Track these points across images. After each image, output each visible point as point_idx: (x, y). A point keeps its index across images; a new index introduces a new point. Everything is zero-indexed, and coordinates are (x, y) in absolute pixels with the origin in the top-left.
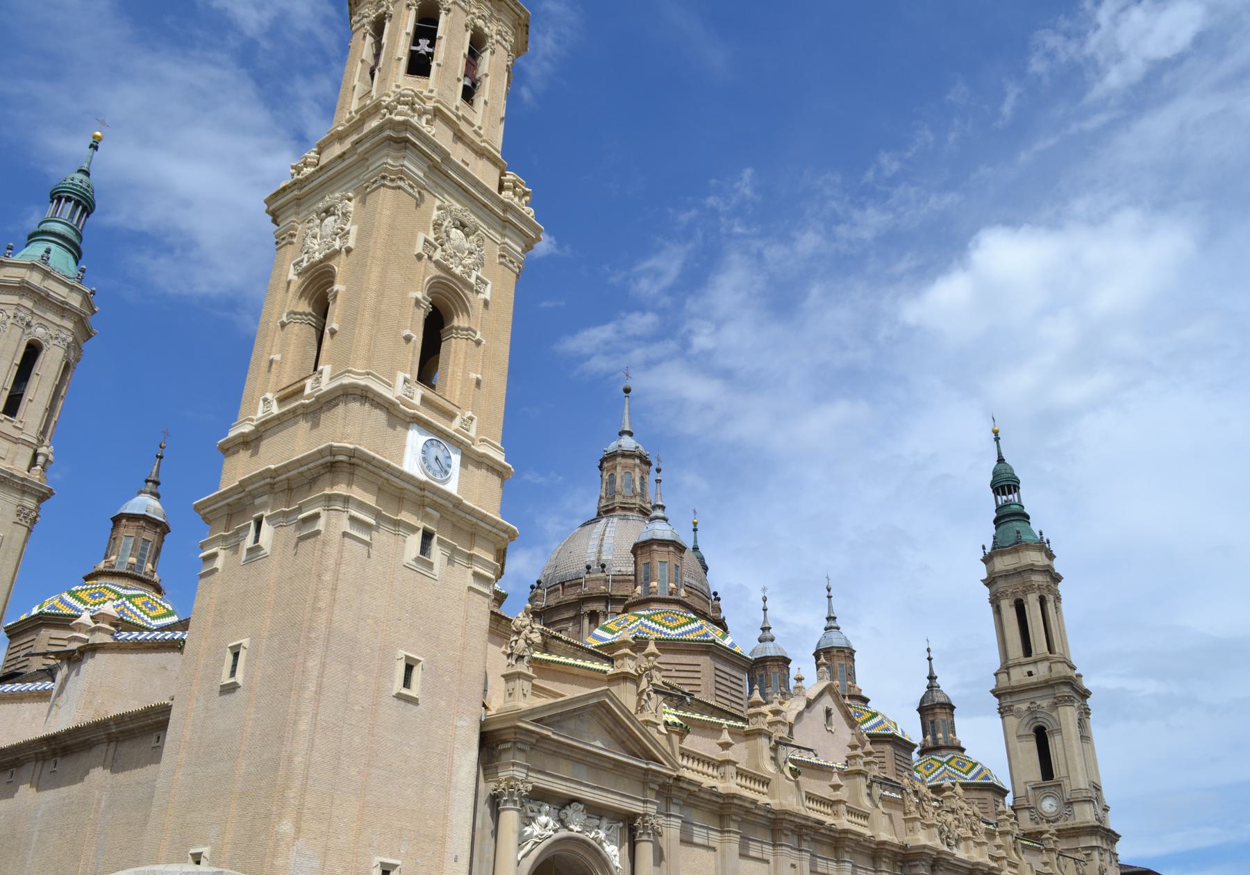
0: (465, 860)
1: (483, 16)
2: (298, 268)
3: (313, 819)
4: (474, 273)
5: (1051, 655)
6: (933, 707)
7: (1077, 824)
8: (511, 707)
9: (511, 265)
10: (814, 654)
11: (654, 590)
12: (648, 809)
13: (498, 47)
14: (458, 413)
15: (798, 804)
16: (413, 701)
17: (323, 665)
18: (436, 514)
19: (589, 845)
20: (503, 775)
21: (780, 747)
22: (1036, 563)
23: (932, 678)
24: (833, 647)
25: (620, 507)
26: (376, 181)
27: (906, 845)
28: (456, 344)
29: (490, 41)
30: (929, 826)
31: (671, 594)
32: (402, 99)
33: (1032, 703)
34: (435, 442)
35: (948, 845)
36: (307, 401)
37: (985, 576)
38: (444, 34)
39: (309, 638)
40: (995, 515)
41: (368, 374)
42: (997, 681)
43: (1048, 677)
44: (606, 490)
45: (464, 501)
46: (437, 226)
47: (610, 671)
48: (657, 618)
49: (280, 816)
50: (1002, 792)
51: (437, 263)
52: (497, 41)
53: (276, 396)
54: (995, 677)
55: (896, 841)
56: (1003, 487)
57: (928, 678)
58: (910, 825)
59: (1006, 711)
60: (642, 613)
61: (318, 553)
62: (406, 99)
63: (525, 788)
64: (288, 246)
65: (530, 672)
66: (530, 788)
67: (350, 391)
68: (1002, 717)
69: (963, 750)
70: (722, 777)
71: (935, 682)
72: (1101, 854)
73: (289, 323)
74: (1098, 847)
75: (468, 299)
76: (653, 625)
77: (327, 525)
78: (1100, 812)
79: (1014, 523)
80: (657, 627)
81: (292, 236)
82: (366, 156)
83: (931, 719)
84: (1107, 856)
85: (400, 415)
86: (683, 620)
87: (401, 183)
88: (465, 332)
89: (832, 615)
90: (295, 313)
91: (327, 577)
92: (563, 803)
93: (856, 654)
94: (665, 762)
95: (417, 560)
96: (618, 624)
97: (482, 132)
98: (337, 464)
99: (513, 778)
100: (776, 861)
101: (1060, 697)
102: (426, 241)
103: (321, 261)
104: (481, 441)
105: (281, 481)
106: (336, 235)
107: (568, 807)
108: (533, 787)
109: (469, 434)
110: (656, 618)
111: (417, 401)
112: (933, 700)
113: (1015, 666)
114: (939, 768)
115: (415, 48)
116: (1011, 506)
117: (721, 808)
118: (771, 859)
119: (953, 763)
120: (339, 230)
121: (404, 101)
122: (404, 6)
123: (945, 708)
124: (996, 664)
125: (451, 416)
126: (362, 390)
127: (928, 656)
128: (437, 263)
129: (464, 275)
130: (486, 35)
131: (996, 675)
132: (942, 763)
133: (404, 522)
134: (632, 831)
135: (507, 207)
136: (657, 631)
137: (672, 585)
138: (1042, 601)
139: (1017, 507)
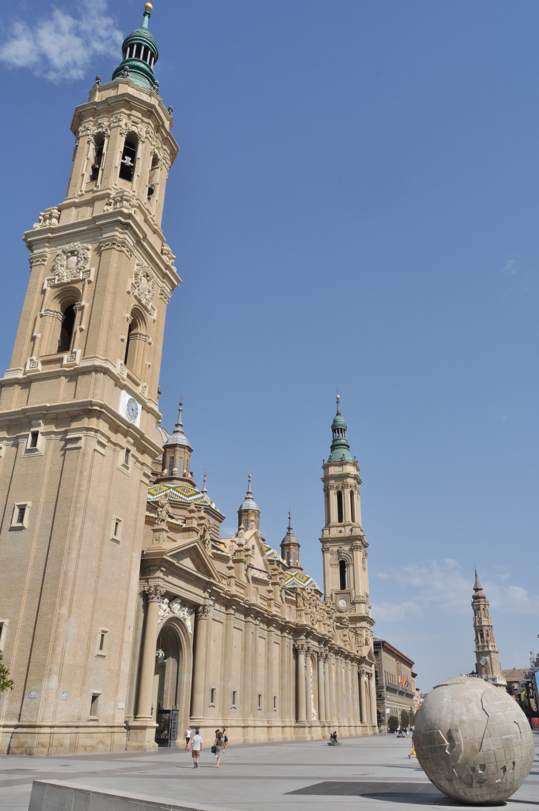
0: (132, 629)
1: (158, 147)
2: (51, 283)
3: (76, 607)
4: (151, 304)
5: (353, 523)
6: (289, 545)
7: (356, 614)
8: (158, 547)
9: (165, 300)
10: (238, 512)
11: (175, 473)
12: (206, 603)
13: (163, 167)
14: (141, 384)
15: (256, 600)
16: (118, 542)
17: (83, 523)
18: (132, 441)
19: (181, 621)
20: (152, 583)
21: (250, 569)
22: (351, 473)
24: (250, 509)
26: (109, 244)
27: (297, 624)
28: (139, 343)
29: (160, 163)
30: (306, 614)
31: (184, 476)
32: (124, 197)
33: (340, 548)
34: (132, 400)
35: (312, 624)
36: (67, 369)
37: (322, 476)
38: (141, 156)
39: (75, 507)
40: (331, 444)
41: (107, 360)
42: (323, 534)
43: (350, 535)
45: (145, 435)
46: (136, 275)
47: (184, 526)
48: (178, 489)
49: (61, 605)
50: (321, 594)
51: (136, 297)
52: (163, 164)
53: (41, 360)
55: (293, 621)
56: (338, 429)
58: (299, 612)
59: (326, 550)
60: (170, 485)
61: (80, 460)
62: (127, 198)
63: (163, 591)
64: (42, 266)
65: (166, 528)
66: (165, 591)
67: (98, 369)
68: (323, 553)
69: (302, 569)
70: (228, 585)
72: (367, 631)
74: (366, 628)
75: (147, 318)
76: (177, 494)
77: (86, 444)
78: (367, 609)
79: (342, 449)
80: (179, 495)
81: (44, 260)
82: (101, 227)
83: (288, 551)
84: (369, 632)
85: (119, 384)
86: (193, 493)
87: (123, 249)
88: (144, 337)
89: (250, 491)
90: (50, 311)
91: (86, 474)
92: (172, 597)
94: (216, 578)
95: (123, 465)
96: (156, 490)
97: (154, 218)
98: (93, 411)
99: (159, 585)
100: (246, 630)
101: (355, 546)
102: (132, 284)
103: (68, 283)
104: (149, 399)
105: (52, 413)
106: (80, 270)
107: (174, 600)
108: (167, 591)
109: (144, 395)
110: (178, 489)
111: (125, 376)
112: (290, 541)
113: (334, 526)
114: (290, 578)
115: (123, 161)
117: (228, 602)
118: (244, 630)
119: (297, 576)
120: (82, 268)
121: (126, 199)
123: (295, 546)
124: (323, 524)
125: (137, 384)
126: (105, 370)
128: (136, 297)
129: (147, 305)
130: (159, 159)
131: (323, 530)
132: (292, 576)
133: (119, 444)
134: (196, 613)
135: (167, 267)
136: (180, 497)
137: (185, 471)
138: (352, 493)
139: (344, 441)
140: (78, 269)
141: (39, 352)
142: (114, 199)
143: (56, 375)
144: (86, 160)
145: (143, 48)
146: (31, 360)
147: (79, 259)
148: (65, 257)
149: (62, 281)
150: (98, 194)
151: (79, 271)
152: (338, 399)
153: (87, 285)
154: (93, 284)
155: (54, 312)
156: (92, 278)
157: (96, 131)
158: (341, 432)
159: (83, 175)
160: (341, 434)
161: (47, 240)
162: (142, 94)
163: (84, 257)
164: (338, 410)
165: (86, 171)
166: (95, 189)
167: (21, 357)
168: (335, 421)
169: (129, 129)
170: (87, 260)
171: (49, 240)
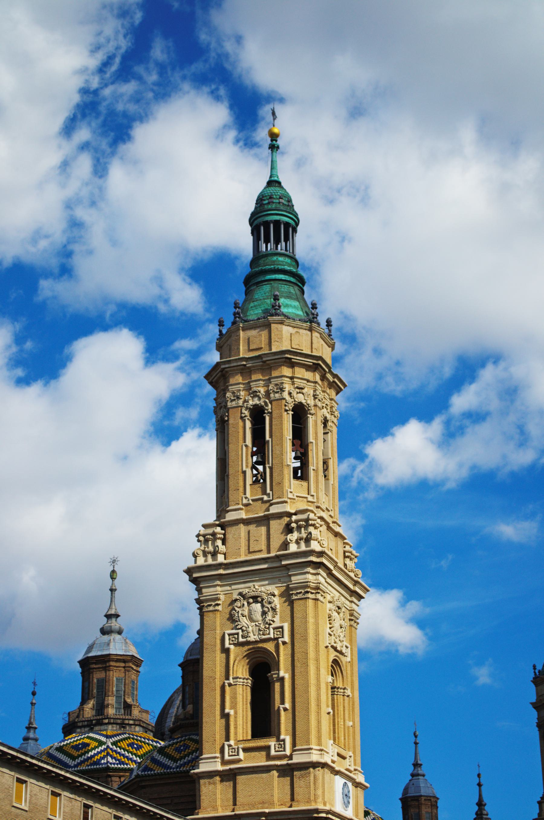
2: (234, 639)
10: (400, 799)
23: (480, 804)
24: (421, 796)
26: (301, 592)
37: (534, 699)
41: (321, 750)
53: (241, 746)
54: (537, 805)
57: (477, 804)
71: (485, 810)
73: (234, 685)
87: (319, 596)
90: (240, 678)
93: (439, 801)
103: (256, 642)
106: (270, 624)
111: (336, 758)
120: (272, 622)
122: (283, 410)
127: (477, 781)
128: (332, 647)
135: (356, 583)
140: (267, 623)
141: (236, 734)
142: (296, 522)
143: (267, 769)
144: (244, 448)
145: (282, 226)
146: (229, 746)
147: (266, 609)
148: (246, 603)
149: (249, 639)
150: (274, 510)
151: (267, 626)
153: (282, 647)
154: (289, 646)
155: (244, 679)
156: (287, 638)
157: (251, 402)
161: (217, 577)
162: (301, 331)
163: (271, 607)
165: (247, 466)
166: (266, 498)
167: (215, 740)
169: (295, 401)
170: (275, 611)
171: (220, 577)
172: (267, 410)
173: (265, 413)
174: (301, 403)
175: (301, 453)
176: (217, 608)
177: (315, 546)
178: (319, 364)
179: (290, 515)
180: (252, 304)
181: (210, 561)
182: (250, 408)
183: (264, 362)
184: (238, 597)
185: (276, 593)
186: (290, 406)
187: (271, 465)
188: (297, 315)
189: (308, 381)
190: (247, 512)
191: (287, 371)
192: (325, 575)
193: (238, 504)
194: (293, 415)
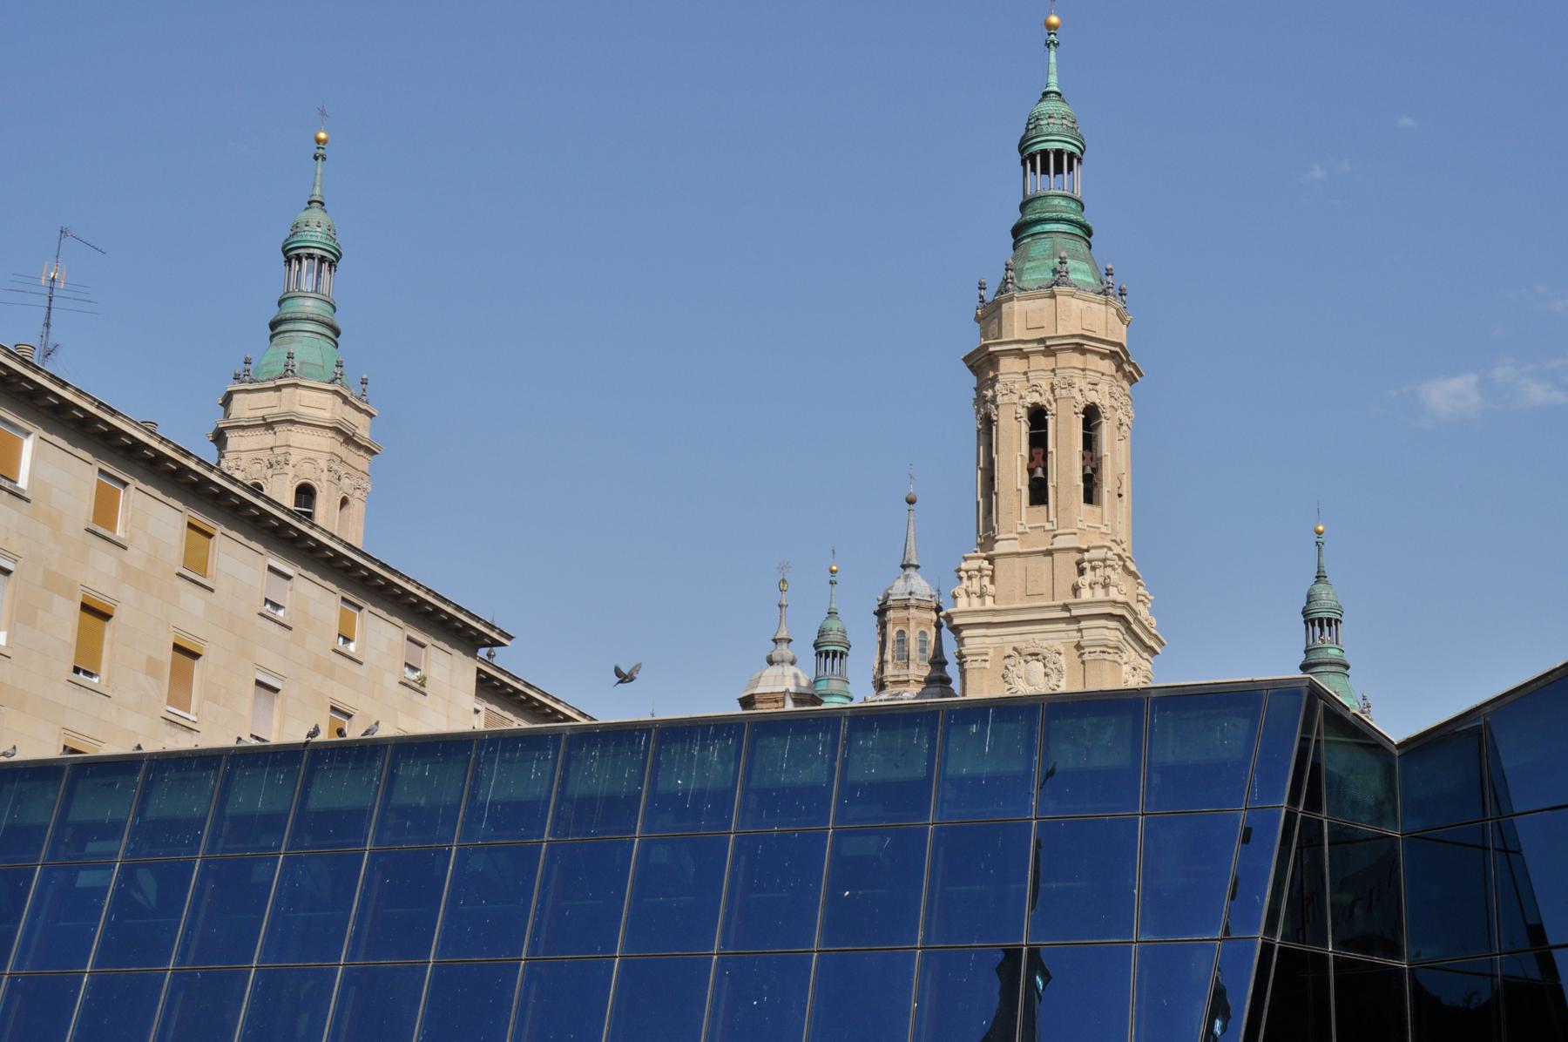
25: (915, 681)
44: (893, 651)
79: (1331, 676)
81: (986, 661)
116: (1329, 651)
120: (1056, 688)
142: (1090, 561)
144: (1019, 458)
145: (1065, 157)
147: (1048, 670)
148: (1022, 661)
150: (1060, 543)
152: (1319, 533)
158: (1329, 625)
159: (1020, 490)
160: (1326, 628)
164: (1319, 567)
165: (1022, 484)
166: (1048, 526)
168: (1310, 599)
172: (1051, 411)
173: (1047, 415)
174: (1094, 403)
175: (1092, 469)
176: (984, 664)
177: (1114, 594)
178: (1116, 353)
179: (1081, 551)
180: (1028, 265)
181: (976, 604)
182: (1027, 407)
183: (1047, 347)
184: (1012, 653)
185: (1062, 650)
186: (1080, 408)
187: (1055, 484)
188: (1089, 283)
189: (1103, 374)
190: (1022, 543)
191: (1076, 359)
192: (1123, 630)
193: (1012, 532)
194: (1084, 419)
